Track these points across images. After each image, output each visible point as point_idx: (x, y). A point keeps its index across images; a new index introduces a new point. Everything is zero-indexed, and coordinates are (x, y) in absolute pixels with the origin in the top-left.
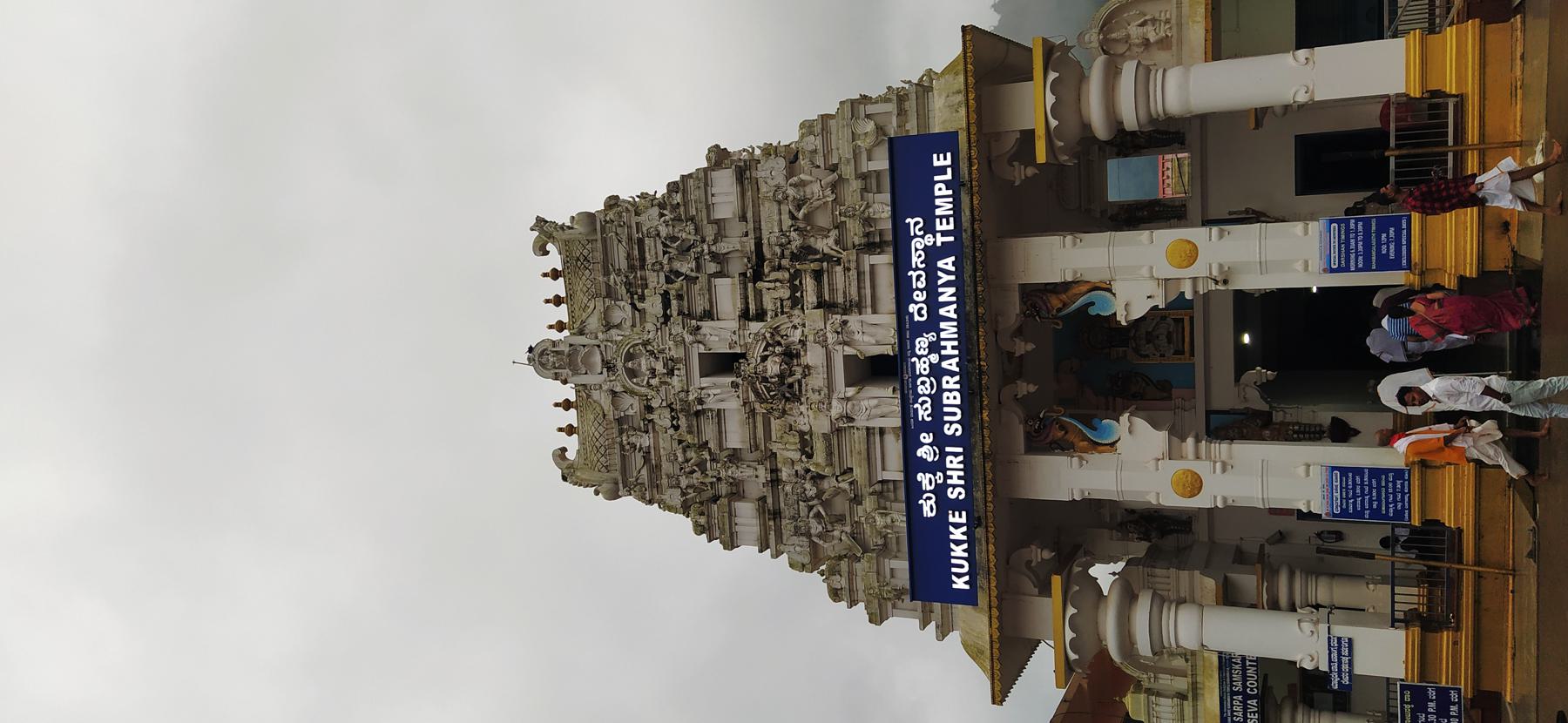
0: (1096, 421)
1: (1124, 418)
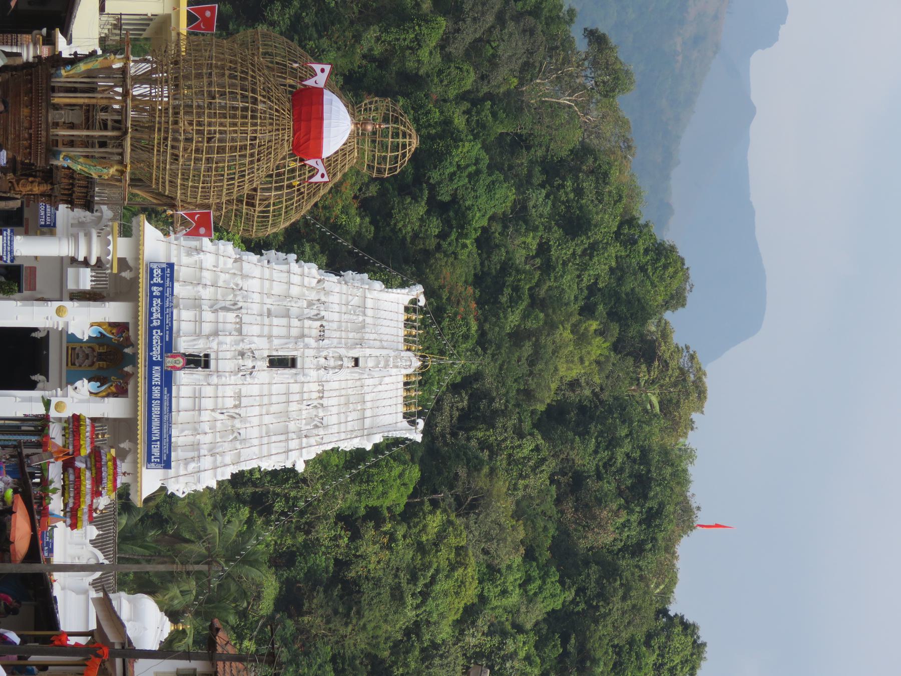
0: (99, 335)
1: (86, 338)
